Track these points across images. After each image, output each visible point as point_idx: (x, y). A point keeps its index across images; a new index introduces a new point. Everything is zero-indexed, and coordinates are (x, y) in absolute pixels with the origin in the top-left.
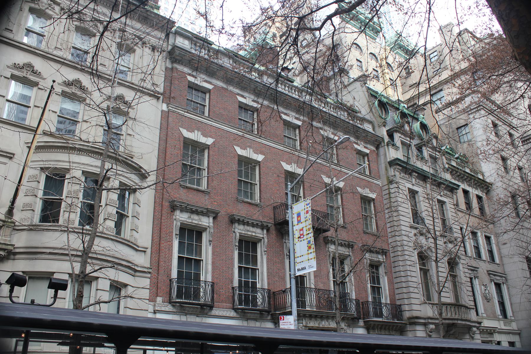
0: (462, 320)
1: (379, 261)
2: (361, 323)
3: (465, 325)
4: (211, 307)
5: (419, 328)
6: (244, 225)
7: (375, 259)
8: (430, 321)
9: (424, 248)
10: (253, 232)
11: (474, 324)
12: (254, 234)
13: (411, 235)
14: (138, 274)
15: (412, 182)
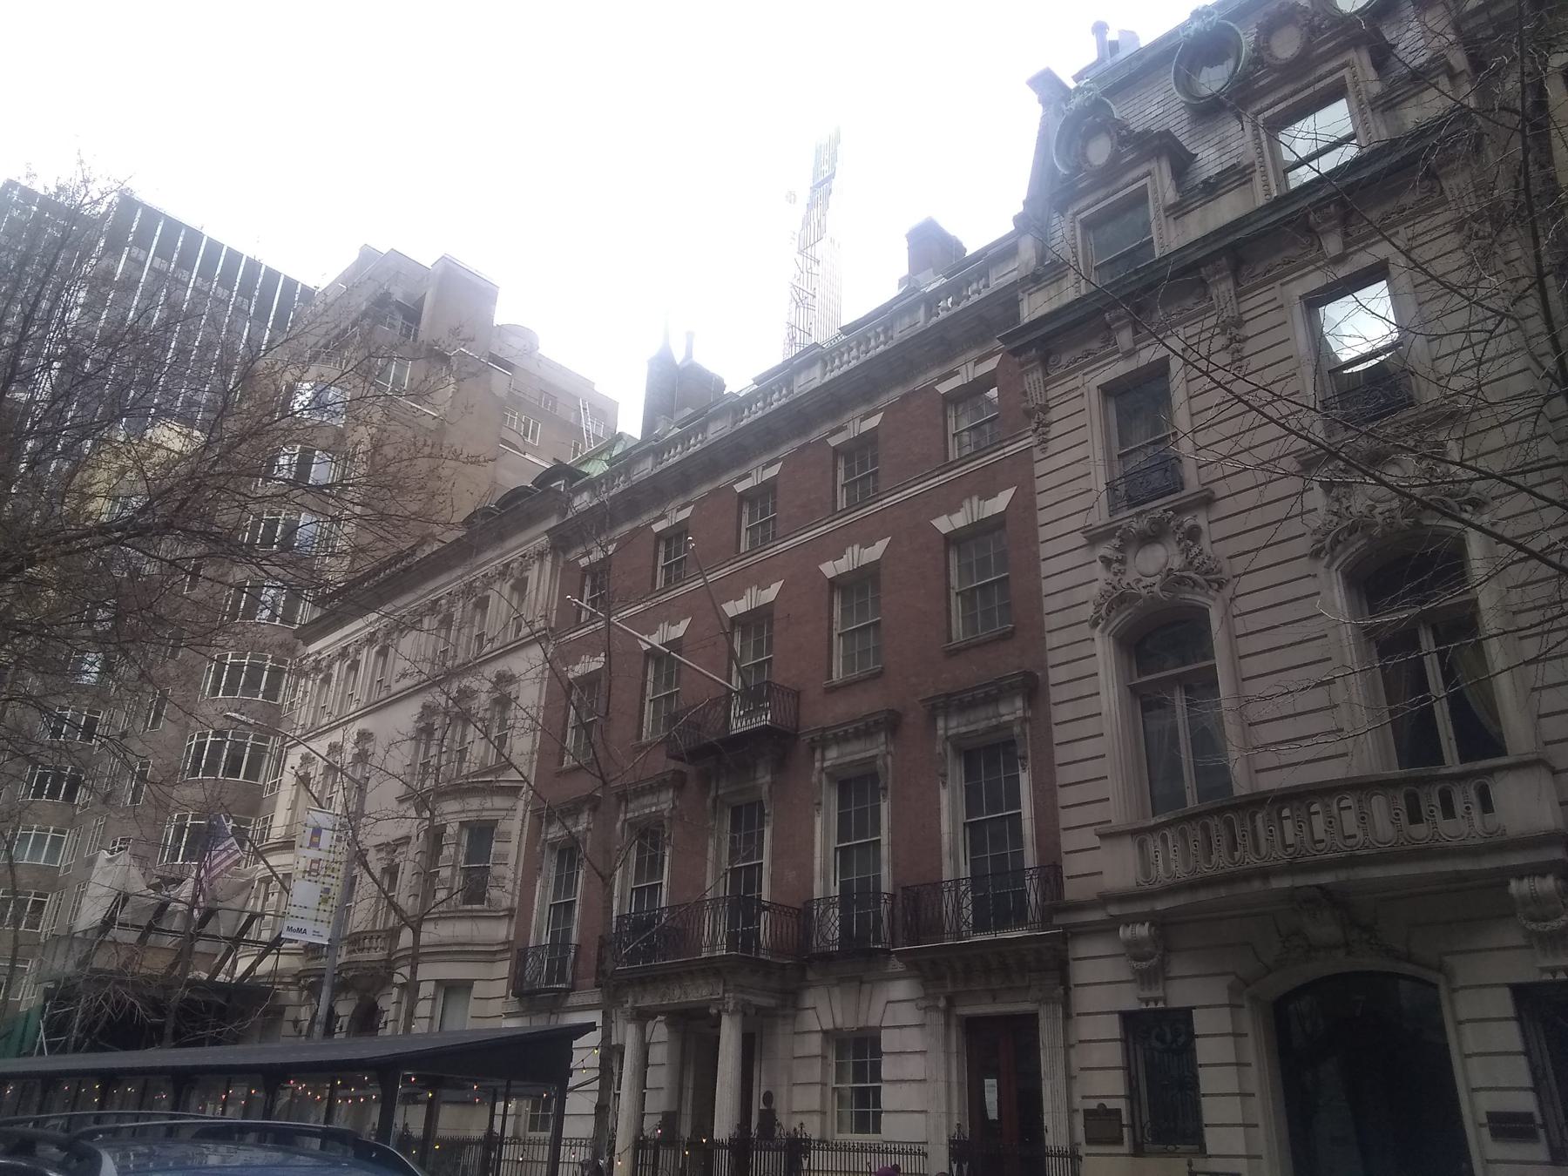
0: (1293, 868)
1: (997, 728)
2: (896, 965)
3: (1460, 877)
4: (568, 992)
5: (1081, 948)
6: (637, 797)
7: (982, 725)
8: (1114, 910)
9: (1144, 592)
10: (651, 806)
11: (1515, 859)
12: (654, 809)
13: (1098, 569)
14: (498, 957)
15: (1117, 351)
